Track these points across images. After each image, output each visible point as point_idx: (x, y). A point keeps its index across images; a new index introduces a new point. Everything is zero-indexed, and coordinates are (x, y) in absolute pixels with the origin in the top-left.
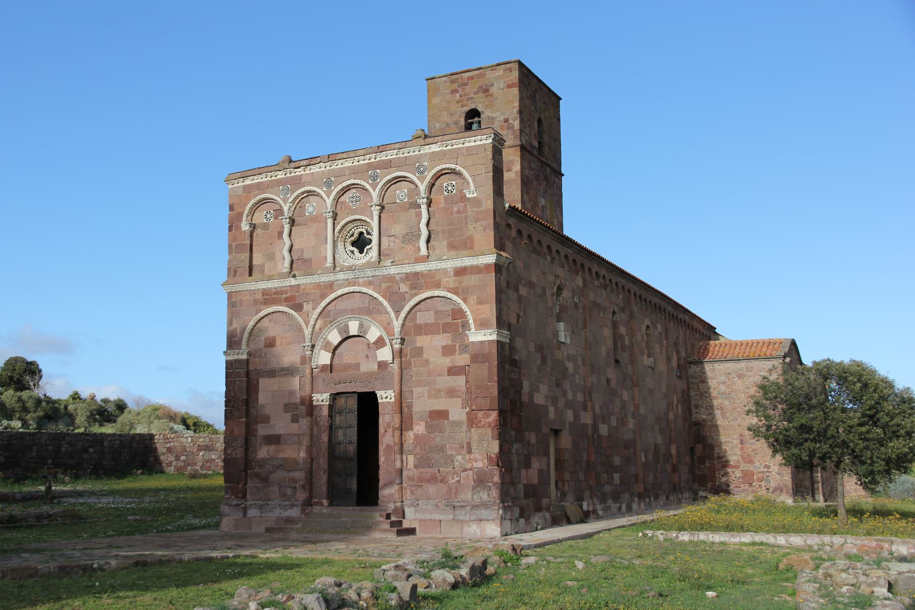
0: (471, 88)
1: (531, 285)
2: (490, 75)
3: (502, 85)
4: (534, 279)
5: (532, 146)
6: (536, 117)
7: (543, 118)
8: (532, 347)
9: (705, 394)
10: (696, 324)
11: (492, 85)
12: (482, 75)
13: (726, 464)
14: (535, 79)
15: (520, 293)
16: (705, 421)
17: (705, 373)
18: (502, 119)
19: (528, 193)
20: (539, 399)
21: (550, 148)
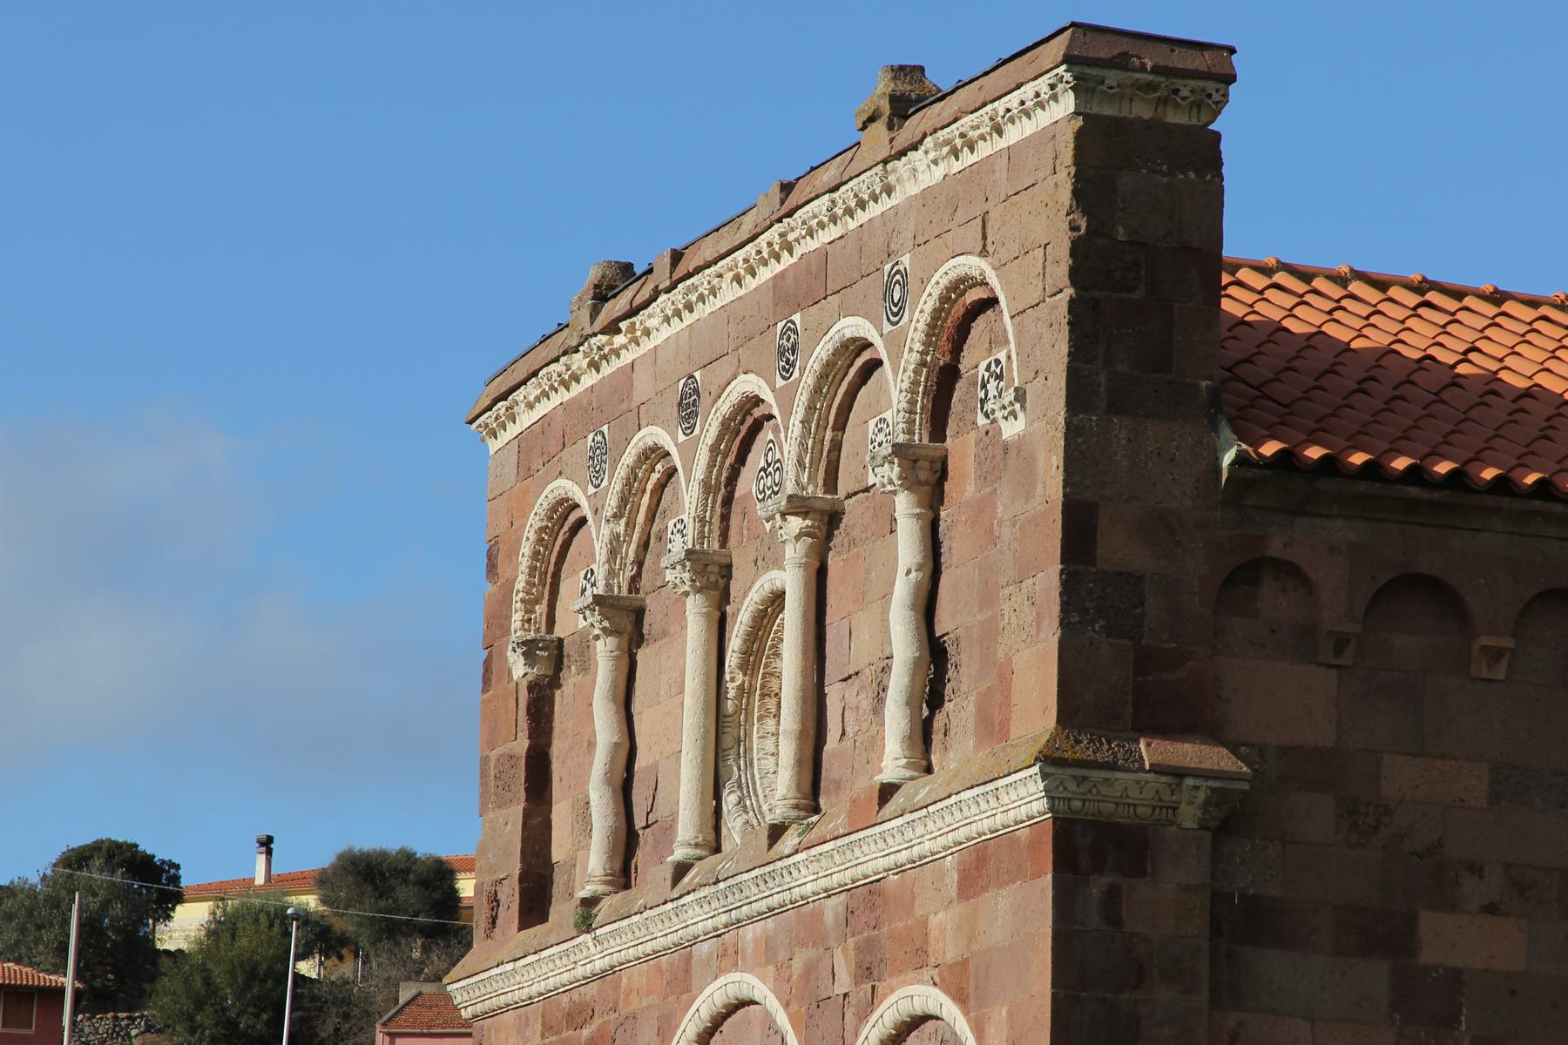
15: (1427, 956)
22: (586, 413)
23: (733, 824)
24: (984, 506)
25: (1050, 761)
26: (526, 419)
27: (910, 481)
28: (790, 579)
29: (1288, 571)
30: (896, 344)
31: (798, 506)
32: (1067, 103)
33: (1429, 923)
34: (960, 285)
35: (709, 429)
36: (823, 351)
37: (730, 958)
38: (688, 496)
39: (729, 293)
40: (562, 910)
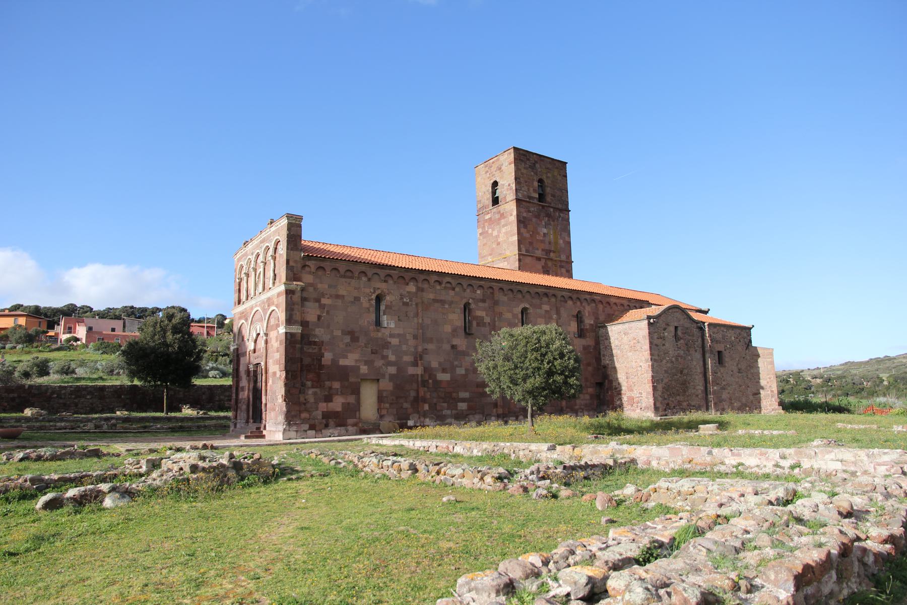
0: (494, 169)
1: (338, 297)
2: (502, 158)
3: (507, 163)
4: (342, 292)
5: (530, 197)
6: (536, 178)
7: (544, 177)
8: (338, 333)
9: (609, 347)
10: (613, 300)
11: (502, 165)
12: (498, 160)
13: (619, 393)
14: (535, 156)
16: (608, 365)
17: (608, 333)
18: (507, 184)
19: (525, 227)
20: (348, 361)
21: (553, 196)
22: (243, 256)
23: (257, 293)
24: (279, 261)
25: (285, 284)
26: (238, 257)
27: (272, 259)
28: (262, 270)
29: (308, 266)
30: (271, 245)
31: (262, 262)
32: (287, 221)
33: (322, 299)
34: (277, 240)
35: (254, 256)
36: (264, 247)
37: (256, 306)
38: (253, 262)
39: (256, 242)
40: (241, 303)
